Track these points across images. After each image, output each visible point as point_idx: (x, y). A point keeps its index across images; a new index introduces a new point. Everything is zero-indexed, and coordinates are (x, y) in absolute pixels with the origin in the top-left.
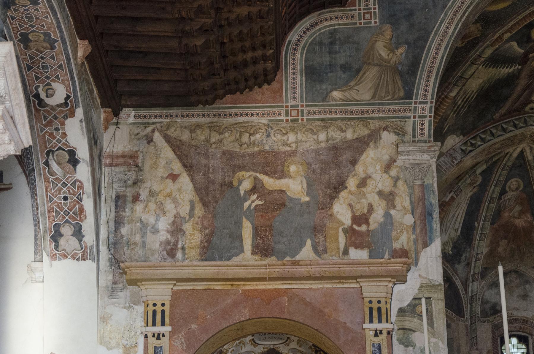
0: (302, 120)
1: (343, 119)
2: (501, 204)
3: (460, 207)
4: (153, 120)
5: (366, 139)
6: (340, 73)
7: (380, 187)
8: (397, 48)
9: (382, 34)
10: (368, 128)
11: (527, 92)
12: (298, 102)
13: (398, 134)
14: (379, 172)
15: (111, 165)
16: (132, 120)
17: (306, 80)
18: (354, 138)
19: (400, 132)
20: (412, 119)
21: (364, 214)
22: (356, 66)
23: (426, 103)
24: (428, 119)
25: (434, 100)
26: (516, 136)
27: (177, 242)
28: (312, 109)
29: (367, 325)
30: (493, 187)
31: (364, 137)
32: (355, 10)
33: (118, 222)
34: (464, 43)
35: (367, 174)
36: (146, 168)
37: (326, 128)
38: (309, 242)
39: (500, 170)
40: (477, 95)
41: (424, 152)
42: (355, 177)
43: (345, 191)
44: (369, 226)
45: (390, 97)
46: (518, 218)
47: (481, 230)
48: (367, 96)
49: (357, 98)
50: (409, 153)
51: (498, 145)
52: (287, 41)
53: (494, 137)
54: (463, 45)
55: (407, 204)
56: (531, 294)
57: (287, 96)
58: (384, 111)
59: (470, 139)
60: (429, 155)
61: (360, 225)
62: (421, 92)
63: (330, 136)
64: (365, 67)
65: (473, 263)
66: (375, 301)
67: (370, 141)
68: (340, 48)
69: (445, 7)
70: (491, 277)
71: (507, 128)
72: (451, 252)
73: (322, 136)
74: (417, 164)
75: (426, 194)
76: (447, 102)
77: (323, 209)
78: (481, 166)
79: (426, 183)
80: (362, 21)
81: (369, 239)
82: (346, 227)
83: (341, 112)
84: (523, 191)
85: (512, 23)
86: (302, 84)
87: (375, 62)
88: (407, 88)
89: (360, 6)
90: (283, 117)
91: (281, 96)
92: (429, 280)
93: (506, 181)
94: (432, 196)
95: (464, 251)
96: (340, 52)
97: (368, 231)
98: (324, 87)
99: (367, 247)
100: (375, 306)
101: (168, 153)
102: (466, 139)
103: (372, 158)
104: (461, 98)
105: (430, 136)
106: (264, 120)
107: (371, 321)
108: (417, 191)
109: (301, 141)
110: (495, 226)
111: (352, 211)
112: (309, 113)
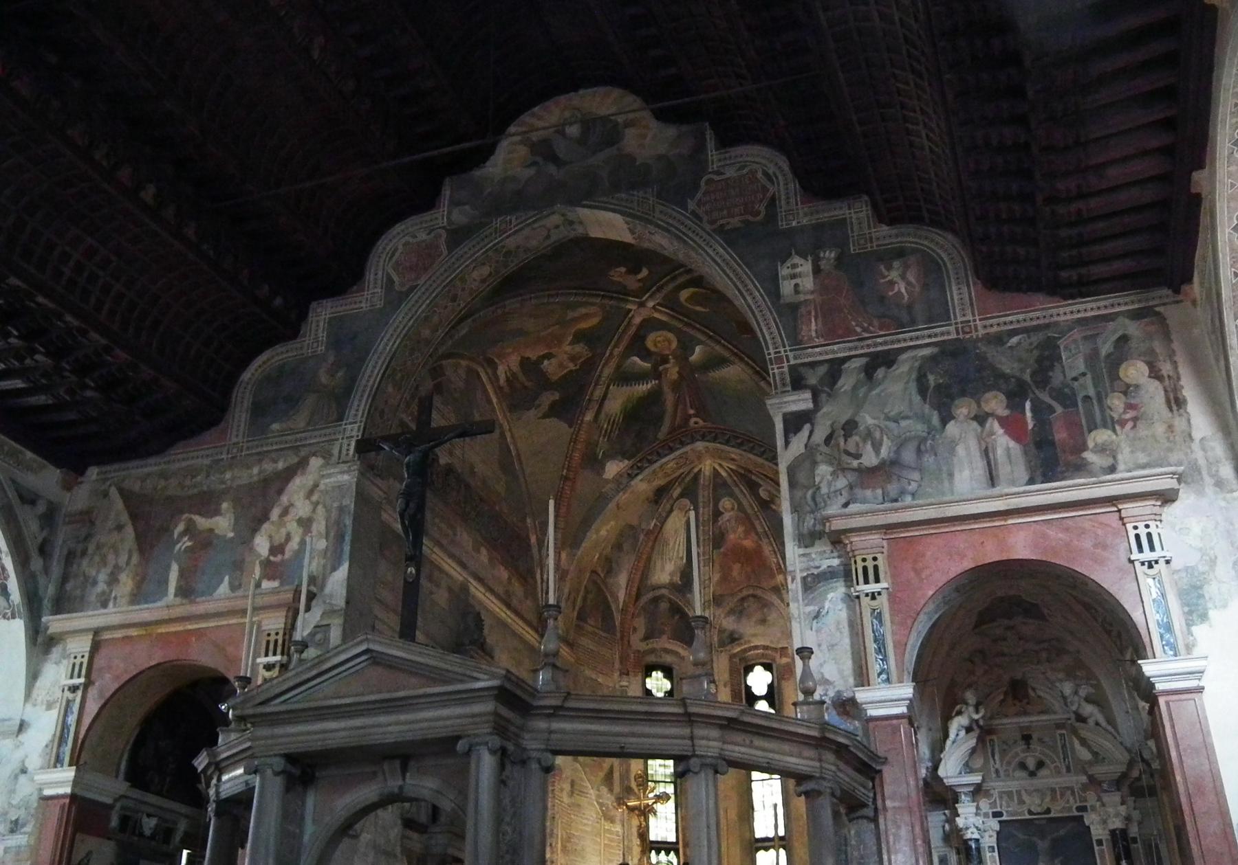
1: (277, 450)
4: (113, 475)
8: (337, 372)
11: (680, 407)
13: (324, 458)
15: (69, 523)
16: (94, 477)
23: (355, 423)
25: (364, 419)
27: (111, 591)
28: (250, 444)
33: (65, 579)
36: (97, 523)
37: (260, 461)
38: (227, 578)
41: (342, 473)
48: (302, 424)
50: (329, 476)
55: (322, 528)
61: (275, 556)
62: (353, 412)
66: (273, 633)
73: (255, 470)
93: (716, 501)
97: (283, 561)
100: (272, 638)
101: (119, 504)
106: (207, 462)
107: (267, 655)
110: (722, 550)
112: (248, 448)
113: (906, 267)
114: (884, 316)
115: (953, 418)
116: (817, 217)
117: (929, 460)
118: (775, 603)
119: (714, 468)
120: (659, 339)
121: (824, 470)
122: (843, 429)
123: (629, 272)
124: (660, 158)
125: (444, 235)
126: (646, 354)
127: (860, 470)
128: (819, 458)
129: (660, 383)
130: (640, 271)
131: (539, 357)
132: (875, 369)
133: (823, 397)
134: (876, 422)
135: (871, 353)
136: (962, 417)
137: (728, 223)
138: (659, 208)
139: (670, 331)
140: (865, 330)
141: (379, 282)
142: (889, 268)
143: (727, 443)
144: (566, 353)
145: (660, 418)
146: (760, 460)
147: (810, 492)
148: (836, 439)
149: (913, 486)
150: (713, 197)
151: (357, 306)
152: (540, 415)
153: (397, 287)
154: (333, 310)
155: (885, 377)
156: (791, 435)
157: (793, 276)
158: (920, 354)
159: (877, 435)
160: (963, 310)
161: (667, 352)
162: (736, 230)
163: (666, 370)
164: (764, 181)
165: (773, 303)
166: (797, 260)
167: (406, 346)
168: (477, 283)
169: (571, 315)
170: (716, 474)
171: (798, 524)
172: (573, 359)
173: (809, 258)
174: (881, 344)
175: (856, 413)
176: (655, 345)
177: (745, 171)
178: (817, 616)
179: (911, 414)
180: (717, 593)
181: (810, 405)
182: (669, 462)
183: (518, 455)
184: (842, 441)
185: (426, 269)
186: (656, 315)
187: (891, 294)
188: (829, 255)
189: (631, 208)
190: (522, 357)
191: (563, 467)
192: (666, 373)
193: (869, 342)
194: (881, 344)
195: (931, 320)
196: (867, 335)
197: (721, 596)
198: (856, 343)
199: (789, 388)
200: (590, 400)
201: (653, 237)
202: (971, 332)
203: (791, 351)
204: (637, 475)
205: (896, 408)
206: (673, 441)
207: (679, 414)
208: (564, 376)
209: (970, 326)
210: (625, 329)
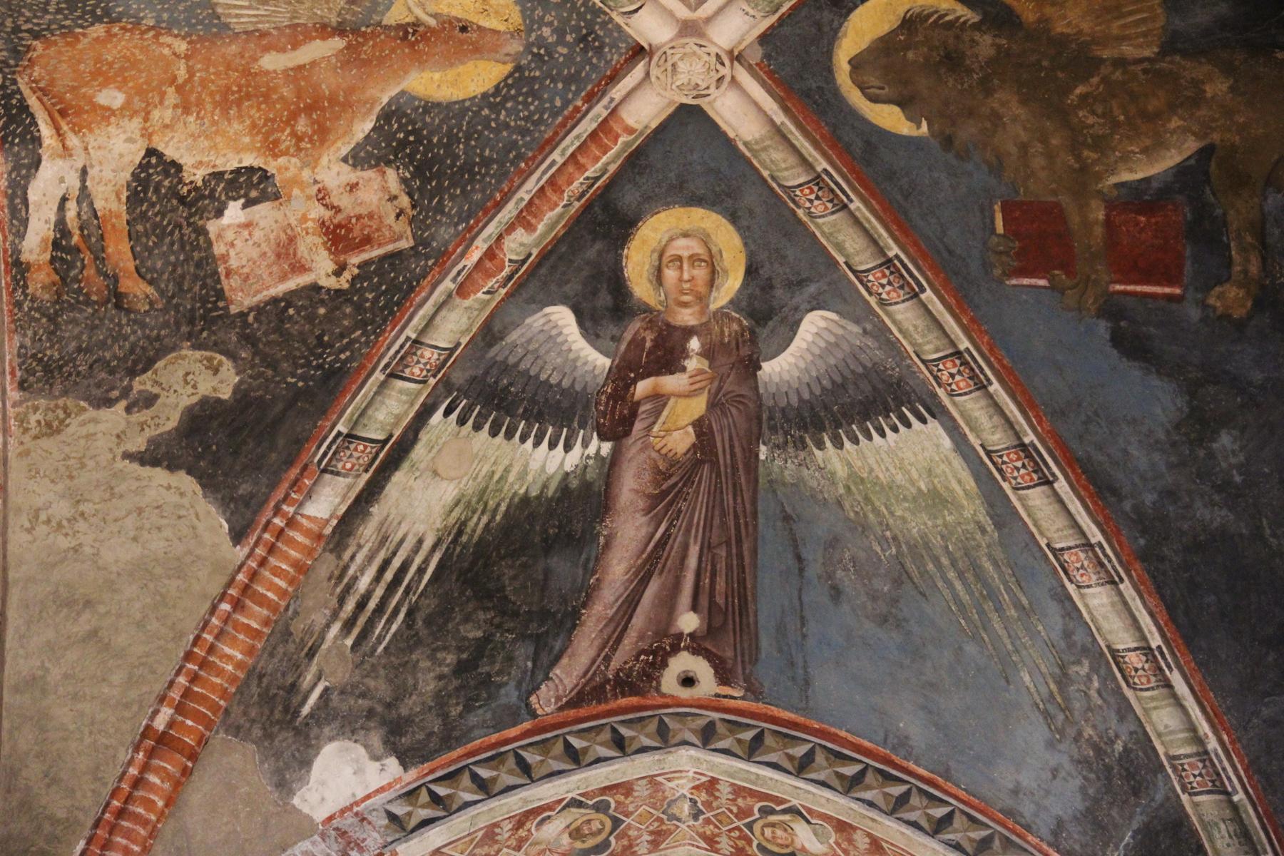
26: (625, 788)
34: (347, 275)
40: (441, 566)
53: (530, 777)
54: (344, 283)
59: (430, 782)
71: (585, 751)
76: (291, 542)
85: (531, 185)
102: (411, 776)
104: (370, 559)
120: (683, 247)
131: (218, 176)
139: (733, 218)
143: (802, 767)
144: (322, 196)
145: (570, 620)
152: (138, 443)
161: (687, 317)
163: (659, 399)
190: (151, 152)
191: (162, 699)
192: (657, 413)
200: (351, 436)
204: (426, 823)
206: (579, 733)
207: (639, 620)
208: (277, 308)
210: (582, 148)
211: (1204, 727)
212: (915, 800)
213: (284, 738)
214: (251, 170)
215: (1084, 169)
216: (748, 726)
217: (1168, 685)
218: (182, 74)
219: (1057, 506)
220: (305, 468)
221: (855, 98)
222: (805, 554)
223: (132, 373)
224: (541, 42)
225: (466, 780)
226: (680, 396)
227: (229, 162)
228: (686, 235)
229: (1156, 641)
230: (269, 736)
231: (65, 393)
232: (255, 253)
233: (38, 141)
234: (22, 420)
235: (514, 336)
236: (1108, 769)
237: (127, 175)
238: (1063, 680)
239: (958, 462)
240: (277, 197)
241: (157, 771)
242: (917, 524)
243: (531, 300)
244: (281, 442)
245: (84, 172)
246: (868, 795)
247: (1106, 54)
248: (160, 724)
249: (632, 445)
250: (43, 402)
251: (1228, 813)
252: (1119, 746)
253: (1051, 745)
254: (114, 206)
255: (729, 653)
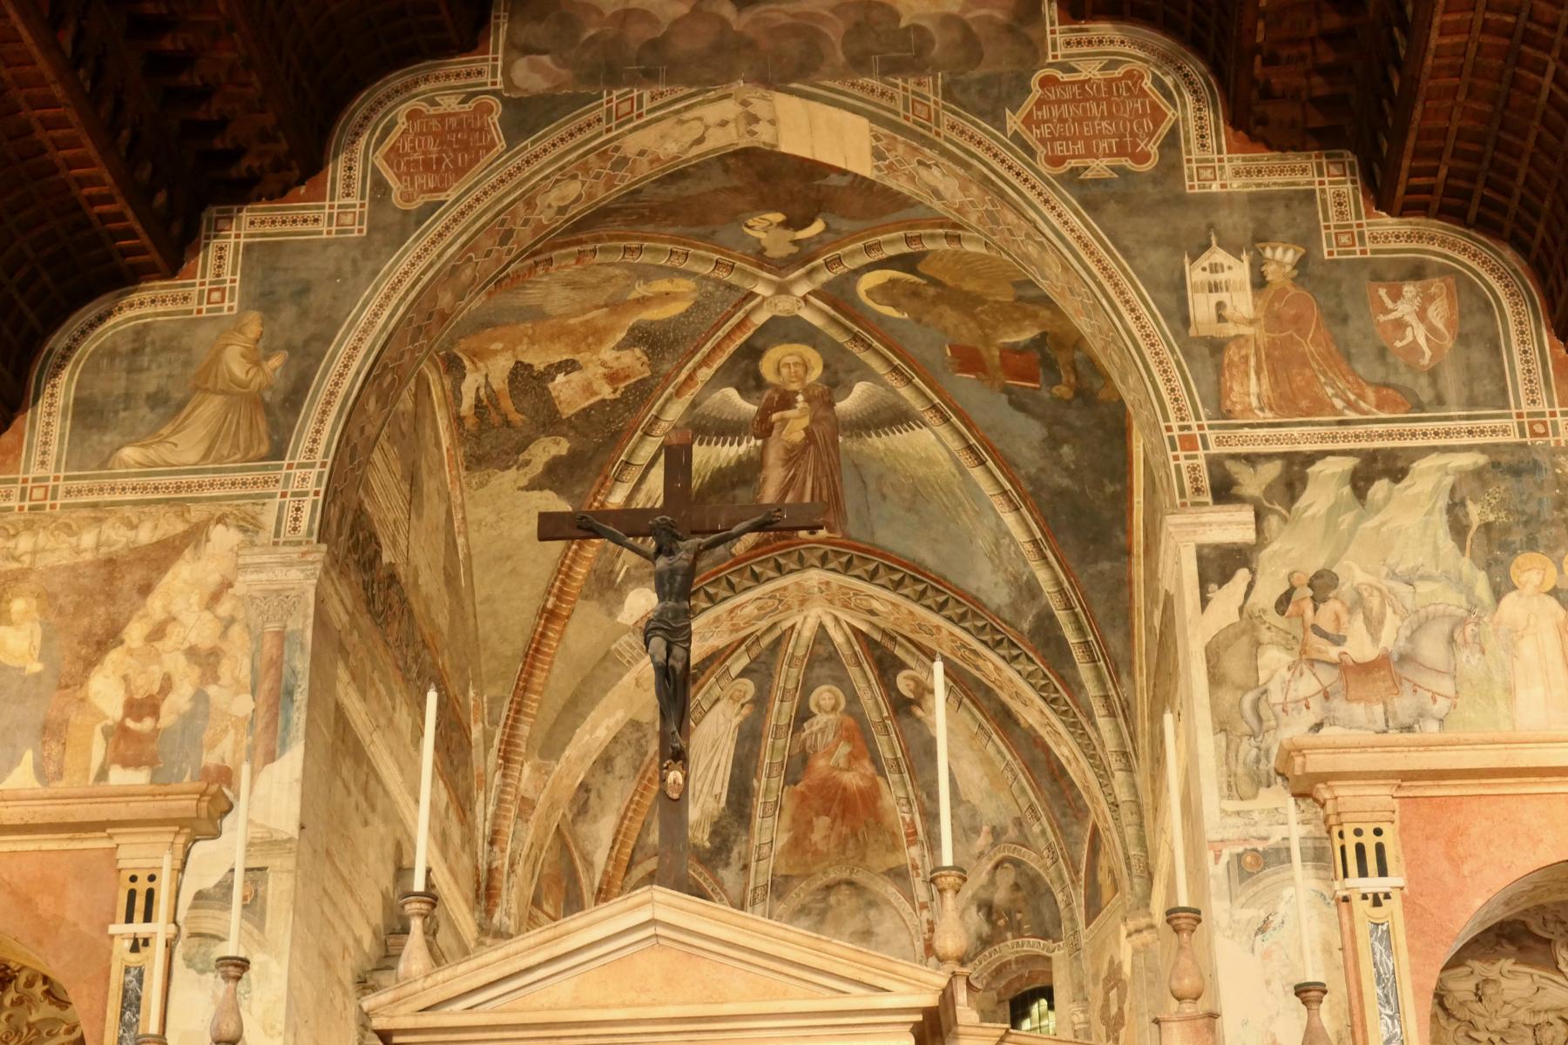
0: (53, 507)
1: (135, 503)
2: (805, 740)
3: (721, 747)
5: (177, 542)
6: (144, 411)
7: (192, 639)
8: (267, 358)
9: (240, 331)
10: (188, 522)
12: (49, 471)
13: (244, 530)
14: (195, 608)
17: (73, 428)
18: (154, 540)
19: (250, 527)
20: (278, 499)
21: (151, 696)
22: (178, 395)
23: (312, 465)
24: (311, 497)
25: (329, 461)
26: (785, 589)
28: (75, 484)
29: (113, 929)
30: (777, 703)
31: (174, 537)
32: (193, 285)
34: (619, 392)
35: (169, 613)
37: (99, 520)
38: (29, 756)
39: (785, 667)
41: (290, 565)
42: (145, 620)
43: (119, 648)
44: (157, 720)
45: (238, 456)
46: (848, 770)
47: (765, 795)
49: (171, 459)
50: (259, 567)
51: (750, 610)
52: (47, 349)
54: (618, 395)
55: (245, 673)
56: (877, 930)
57: (28, 458)
58: (222, 484)
60: (303, 571)
61: (139, 719)
62: (305, 443)
63: (103, 538)
64: (198, 397)
65: (753, 864)
67: (187, 546)
68: (151, 361)
69: (375, 273)
70: (798, 895)
71: (762, 574)
72: (708, 845)
73: (88, 539)
74: (277, 591)
75: (286, 652)
77: (67, 687)
78: (738, 658)
79: (289, 629)
80: (205, 307)
81: (154, 747)
82: (110, 723)
83: (134, 489)
84: (847, 711)
86: (62, 436)
87: (219, 386)
88: (276, 438)
89: (203, 276)
90: (14, 503)
91: (17, 458)
92: (270, 831)
93: (807, 689)
94: (298, 654)
95: (735, 841)
96: (148, 369)
97: (156, 730)
98: (107, 438)
99: (146, 763)
100: (142, 886)
103: (185, 582)
105: (310, 533)
108: (267, 646)
109: (43, 550)
110: (800, 787)
111: (128, 690)
112: (68, 492)
113: (1428, 299)
114: (1387, 386)
115: (1515, 588)
116: (1258, 180)
117: (1469, 660)
118: (892, 900)
119: (822, 626)
120: (789, 360)
121: (1274, 659)
122: (1310, 585)
123: (786, 225)
124: (948, 20)
125: (498, 108)
126: (751, 383)
127: (1340, 665)
128: (1265, 636)
129: (764, 446)
130: (807, 222)
131: (551, 366)
132: (1370, 480)
133: (1273, 522)
134: (1372, 580)
135: (1361, 450)
136: (1529, 589)
137: (1086, 168)
138: (947, 118)
139: (814, 347)
140: (1351, 405)
141: (357, 186)
142: (1396, 296)
143: (872, 577)
144: (603, 364)
146: (935, 619)
147: (1248, 699)
148: (1297, 602)
149: (1441, 706)
150: (1055, 113)
151: (305, 228)
152: (524, 482)
153: (396, 199)
154: (253, 230)
155: (1387, 499)
156: (1213, 587)
157: (1214, 287)
158: (1453, 465)
159: (1375, 602)
160: (1532, 392)
161: (795, 387)
162: (1097, 182)
163: (784, 421)
164: (1156, 96)
165: (1176, 334)
166: (1218, 255)
167: (411, 320)
168: (551, 213)
169: (640, 290)
170: (822, 634)
171: (1228, 755)
172: (612, 378)
173: (1244, 256)
174: (1380, 436)
175: (1335, 560)
176: (778, 371)
177: (1119, 72)
178: (1262, 930)
179: (1436, 573)
180: (783, 872)
181: (1247, 535)
182: (748, 601)
183: (469, 556)
184: (1308, 607)
185: (460, 172)
186: (806, 314)
187: (1398, 344)
188: (1282, 258)
189: (890, 110)
190: (517, 363)
193: (1360, 429)
194: (1380, 436)
195: (1472, 402)
196: (1351, 415)
197: (787, 877)
198: (1335, 429)
199: (1208, 498)
200: (627, 463)
201: (923, 172)
202: (1546, 434)
203: (1211, 427)
205: (1411, 557)
208: (586, 412)
209: (1544, 424)
211: (1062, 576)
212: (929, 593)
213: (610, 595)
214: (567, 361)
215: (986, 336)
216: (846, 554)
217: (1044, 557)
218: (530, 332)
219: (987, 475)
220: (606, 478)
221: (870, 303)
222: (866, 479)
223: (518, 453)
224: (708, 292)
225: (702, 595)
226: (795, 418)
227: (557, 359)
228: (790, 355)
229: (1039, 535)
230: (601, 595)
231: (487, 468)
232: (572, 392)
233: (464, 368)
234: (468, 484)
235: (706, 403)
236: (1020, 589)
237: (507, 373)
238: (997, 544)
239: (939, 446)
240: (580, 368)
241: (552, 630)
242: (922, 471)
243: (714, 387)
244: (594, 467)
245: (487, 376)
246: (905, 591)
247: (990, 298)
248: (549, 605)
249: (773, 440)
250: (477, 474)
251: (1072, 619)
252: (1025, 578)
253: (994, 572)
254: (502, 386)
255: (832, 520)
